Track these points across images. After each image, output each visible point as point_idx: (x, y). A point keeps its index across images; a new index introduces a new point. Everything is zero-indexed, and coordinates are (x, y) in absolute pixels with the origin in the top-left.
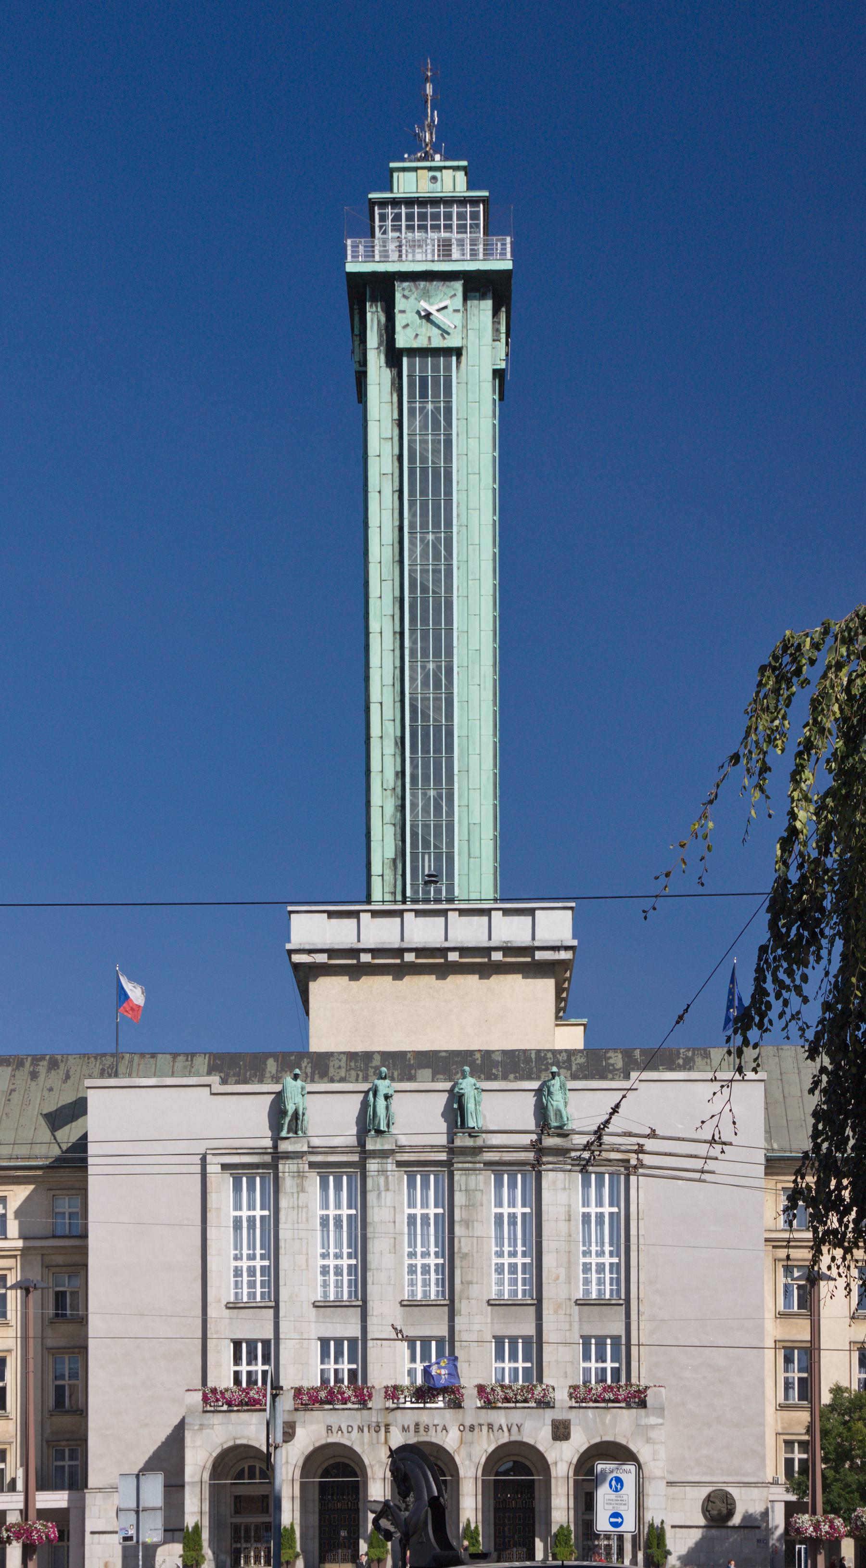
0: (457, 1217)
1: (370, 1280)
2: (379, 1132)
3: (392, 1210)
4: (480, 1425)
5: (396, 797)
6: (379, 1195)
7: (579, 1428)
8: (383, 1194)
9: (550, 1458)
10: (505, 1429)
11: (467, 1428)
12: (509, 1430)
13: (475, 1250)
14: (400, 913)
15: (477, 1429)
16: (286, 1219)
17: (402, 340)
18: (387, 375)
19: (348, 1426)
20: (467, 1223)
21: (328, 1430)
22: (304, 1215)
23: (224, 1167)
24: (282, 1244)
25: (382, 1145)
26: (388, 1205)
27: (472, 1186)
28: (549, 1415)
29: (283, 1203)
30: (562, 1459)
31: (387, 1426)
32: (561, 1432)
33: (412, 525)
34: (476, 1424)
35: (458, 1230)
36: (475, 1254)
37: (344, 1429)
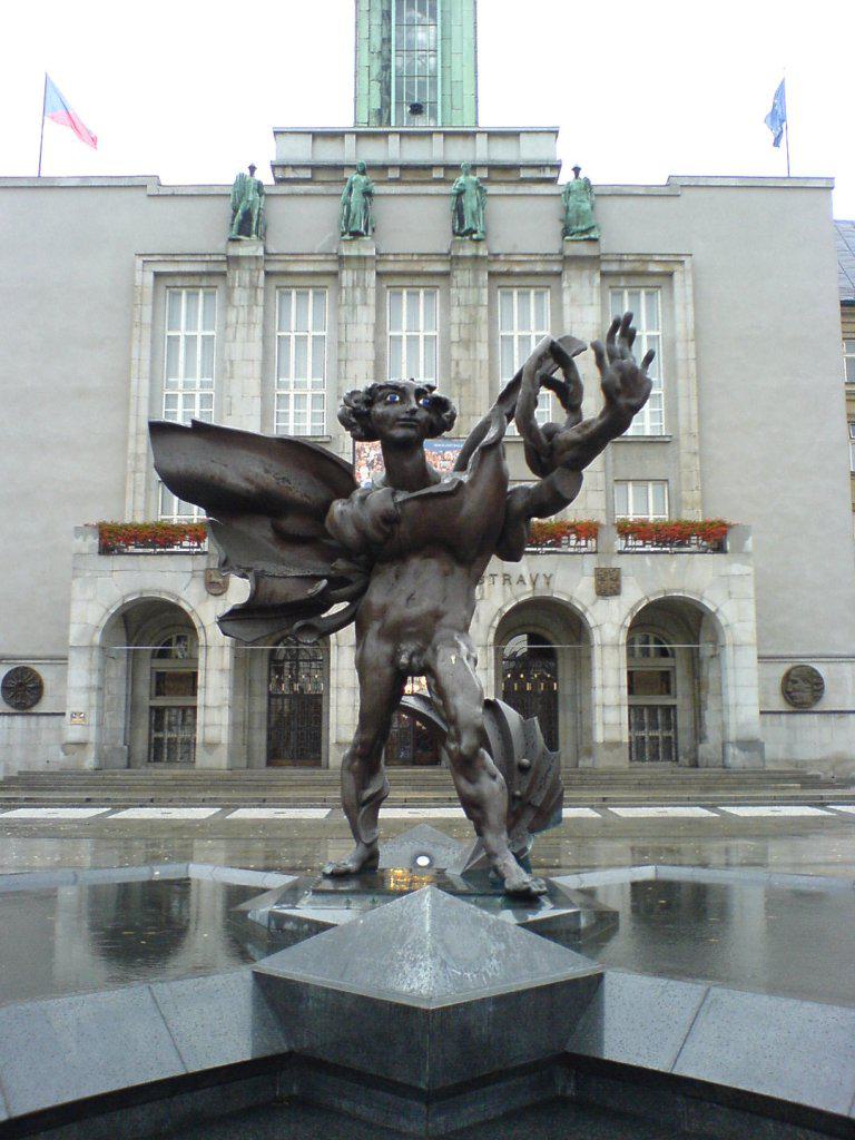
0: (455, 336)
2: (356, 234)
3: (371, 329)
5: (383, 59)
7: (632, 579)
8: (359, 308)
9: (591, 620)
10: (527, 580)
12: (534, 583)
14: (386, 134)
20: (468, 343)
23: (157, 275)
25: (359, 250)
26: (365, 320)
28: (590, 563)
30: (608, 622)
32: (608, 585)
36: (477, 381)
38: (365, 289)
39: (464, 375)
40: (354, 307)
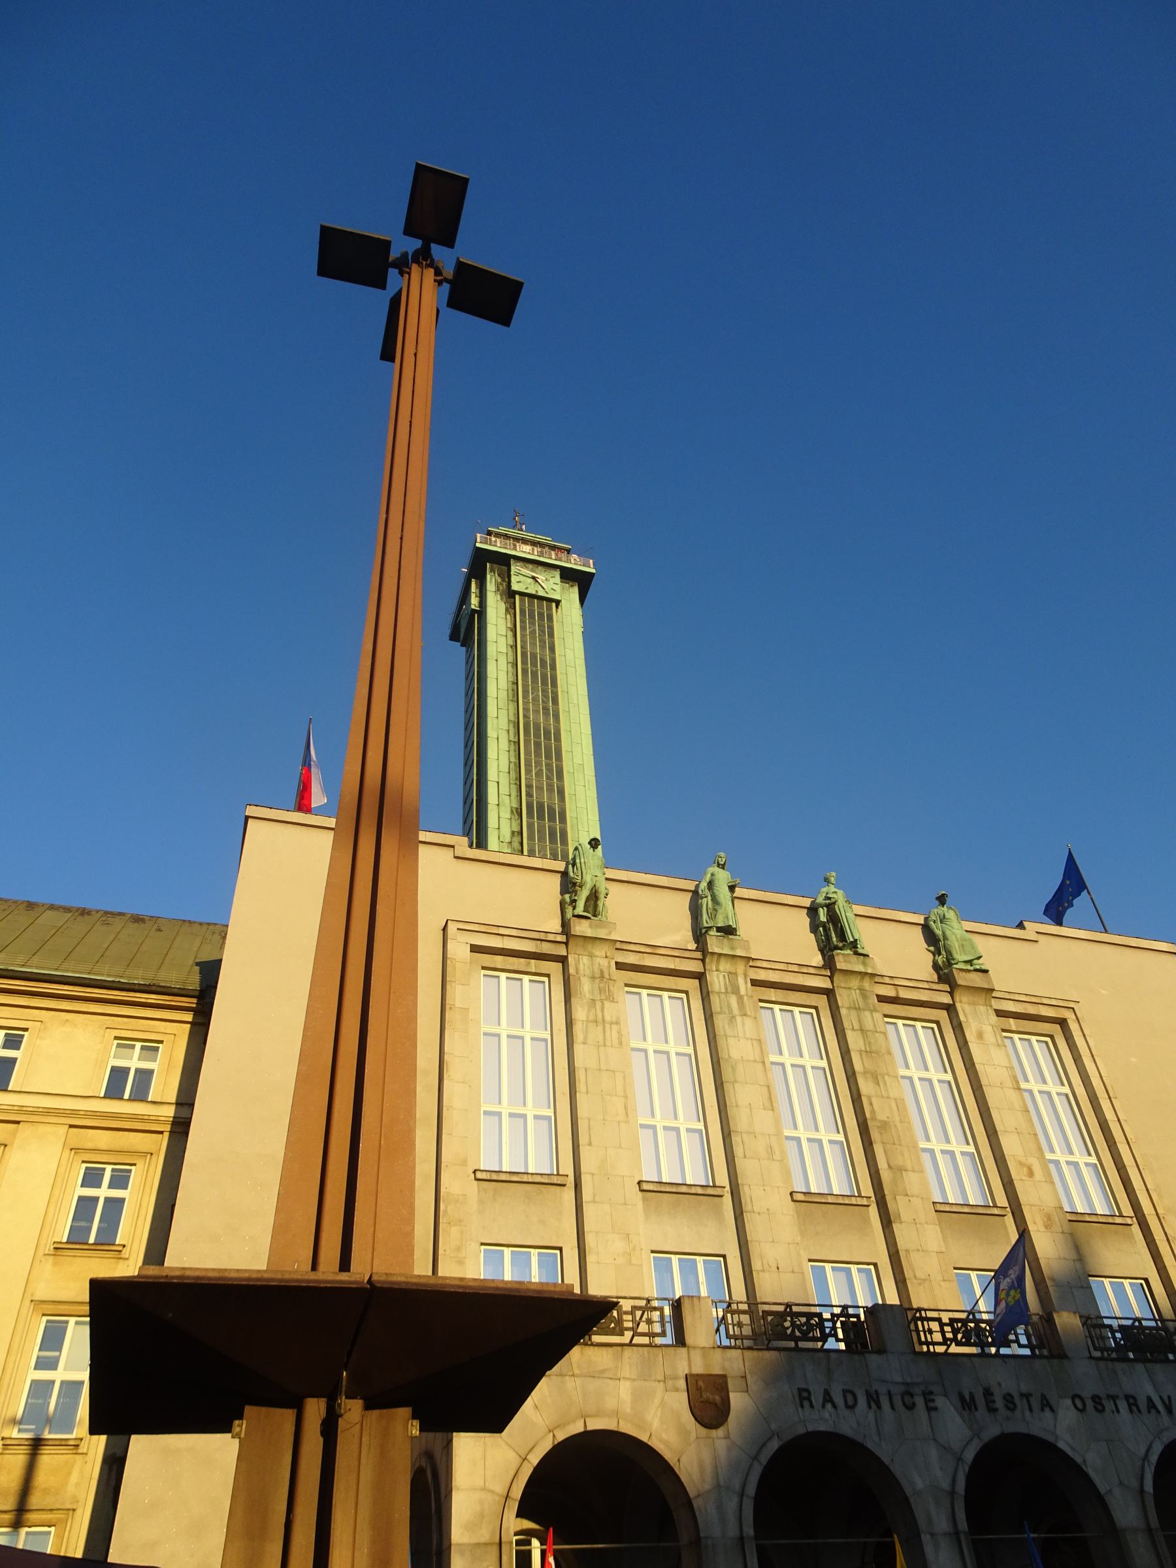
0: (858, 1066)
1: (738, 1151)
3: (755, 1043)
4: (1113, 1398)
6: (732, 1018)
8: (739, 1019)
11: (1090, 1404)
13: (897, 1119)
15: (1109, 1406)
16: (585, 1038)
17: (515, 587)
18: (502, 606)
19: (845, 1392)
21: (802, 1399)
22: (615, 1035)
23: (475, 949)
24: (580, 1075)
27: (869, 1025)
29: (580, 1013)
31: (928, 1396)
33: (525, 687)
34: (1103, 1395)
35: (865, 1086)
36: (898, 1125)
37: (838, 1399)
38: (740, 998)
39: (881, 1116)
40: (733, 1017)
